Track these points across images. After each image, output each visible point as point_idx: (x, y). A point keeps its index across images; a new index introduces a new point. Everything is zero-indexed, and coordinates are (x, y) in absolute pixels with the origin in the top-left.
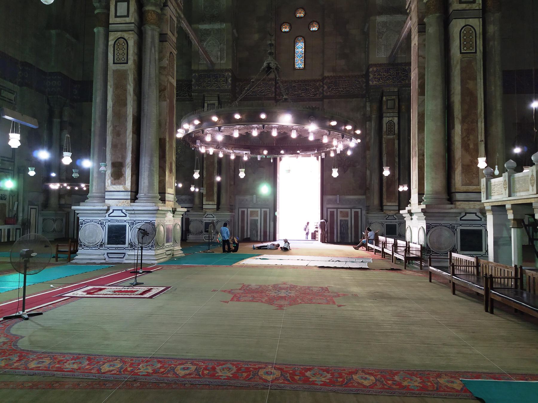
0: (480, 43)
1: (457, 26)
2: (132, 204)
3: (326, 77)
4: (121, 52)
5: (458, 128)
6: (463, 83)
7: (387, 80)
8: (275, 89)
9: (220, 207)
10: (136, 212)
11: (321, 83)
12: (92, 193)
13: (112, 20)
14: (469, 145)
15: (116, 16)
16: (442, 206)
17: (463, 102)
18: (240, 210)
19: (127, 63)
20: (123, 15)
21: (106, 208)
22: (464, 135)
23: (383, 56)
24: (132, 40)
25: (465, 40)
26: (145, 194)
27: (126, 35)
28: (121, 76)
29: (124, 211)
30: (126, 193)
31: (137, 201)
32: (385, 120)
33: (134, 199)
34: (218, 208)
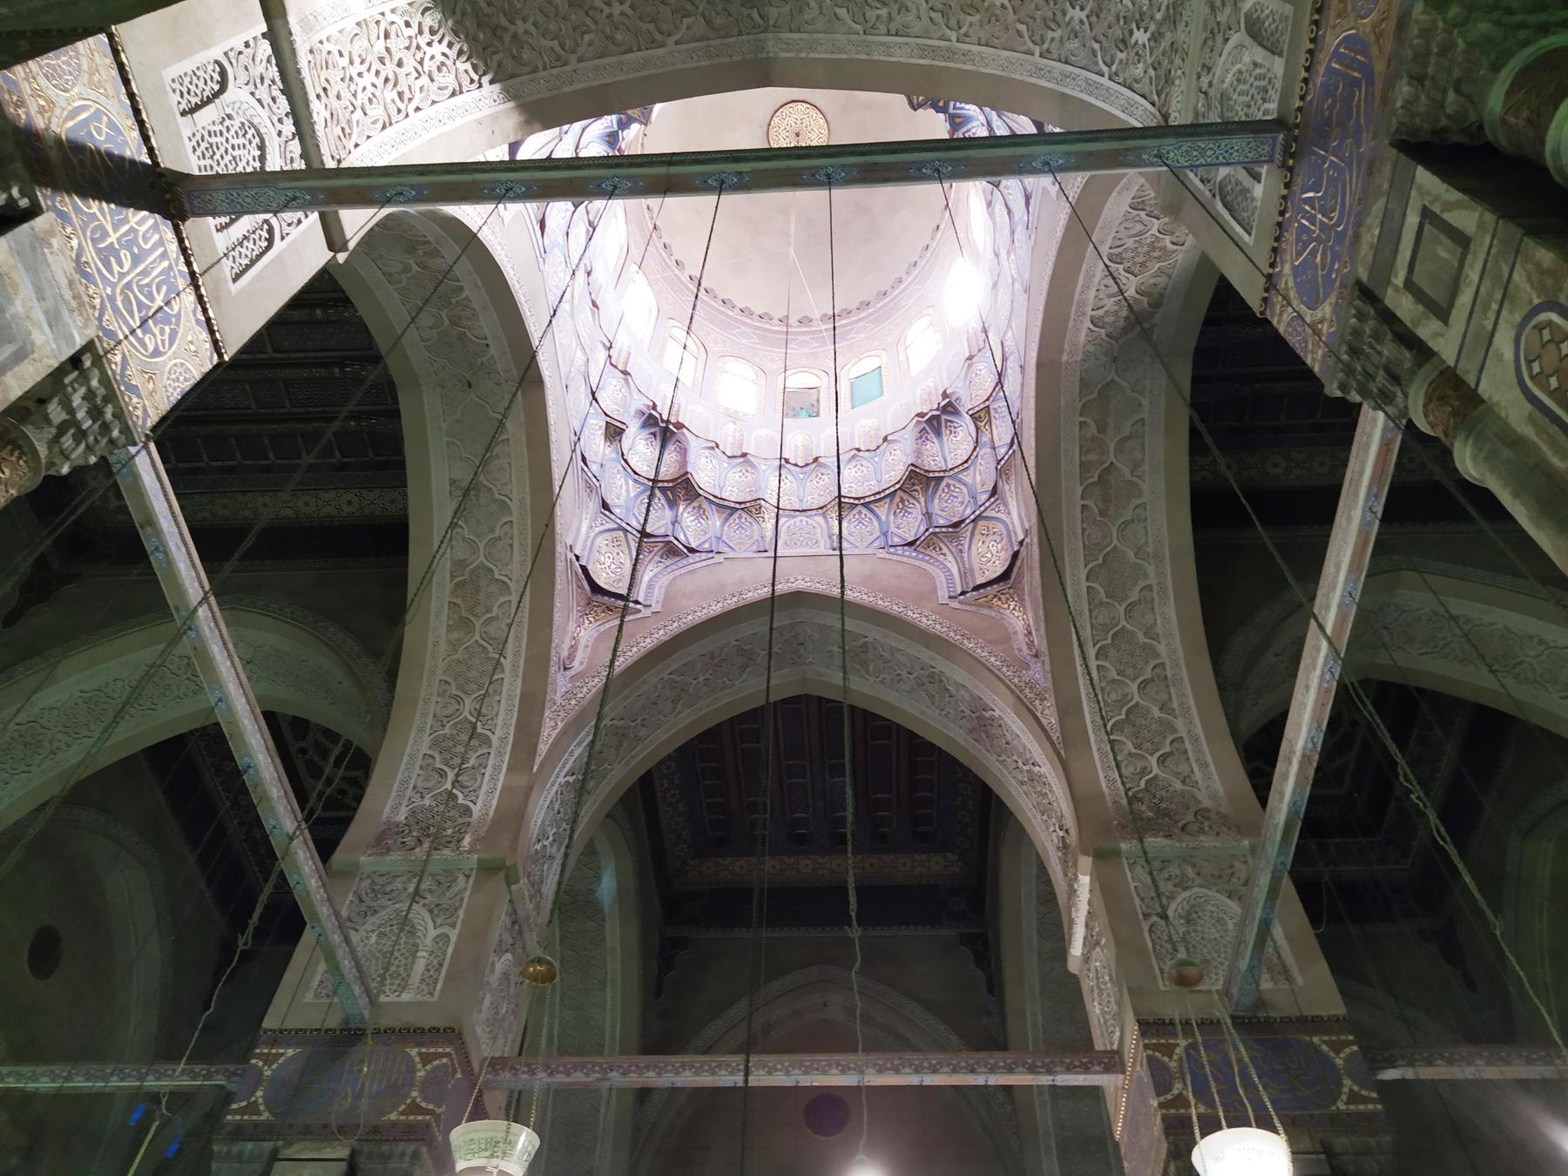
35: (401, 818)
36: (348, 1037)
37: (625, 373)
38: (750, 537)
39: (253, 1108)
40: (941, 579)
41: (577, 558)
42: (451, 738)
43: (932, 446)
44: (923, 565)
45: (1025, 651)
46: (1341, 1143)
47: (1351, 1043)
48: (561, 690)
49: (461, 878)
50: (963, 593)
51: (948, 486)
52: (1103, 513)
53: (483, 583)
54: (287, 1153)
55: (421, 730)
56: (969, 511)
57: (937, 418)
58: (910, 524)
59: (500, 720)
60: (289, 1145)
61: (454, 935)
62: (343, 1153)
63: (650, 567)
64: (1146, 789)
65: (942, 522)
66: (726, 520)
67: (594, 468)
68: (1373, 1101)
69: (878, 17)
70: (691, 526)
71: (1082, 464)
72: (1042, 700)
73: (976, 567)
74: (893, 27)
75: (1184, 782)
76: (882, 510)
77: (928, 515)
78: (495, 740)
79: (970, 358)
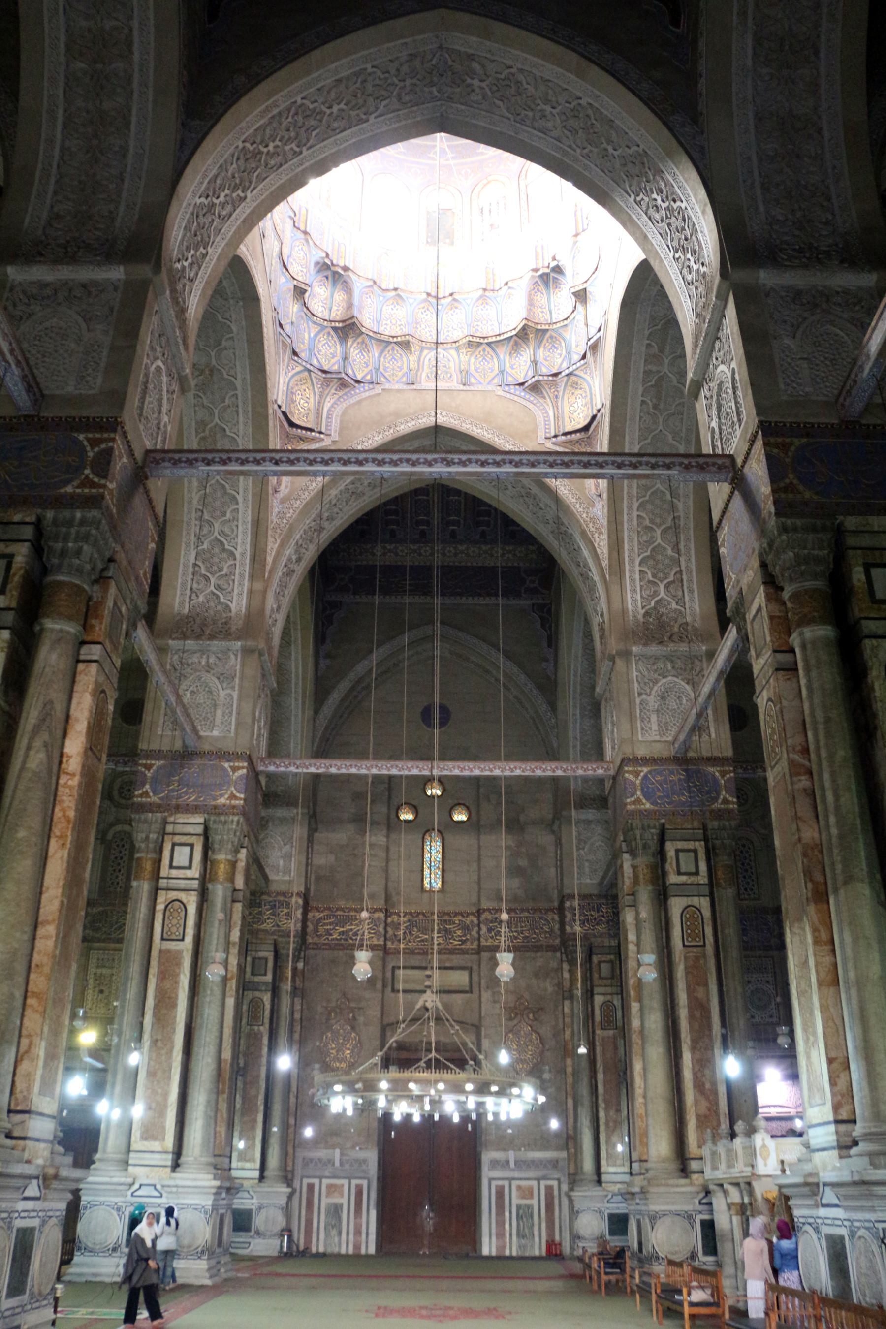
0: (709, 931)
1: (676, 905)
2: (174, 1175)
3: (484, 910)
4: (175, 922)
5: (687, 1058)
6: (690, 991)
7: (598, 924)
8: (385, 929)
9: (266, 1174)
10: (180, 1190)
11: (475, 920)
12: (104, 1151)
13: (164, 872)
14: (703, 1085)
15: (171, 867)
16: (671, 1182)
17: (691, 1017)
18: (306, 1181)
19: (183, 940)
20: (182, 865)
21: (130, 1180)
22: (696, 1069)
23: (588, 881)
24: (192, 902)
25: (688, 927)
26: (196, 1159)
27: (182, 896)
28: (170, 961)
29: (159, 1187)
30: (164, 1156)
31: (178, 1169)
32: (598, 1000)
33: (176, 1166)
34: (262, 1178)
35: (186, 611)
36: (186, 755)
37: (305, 233)
38: (401, 368)
39: (146, 794)
40: (540, 421)
41: (280, 407)
42: (209, 551)
43: (541, 299)
44: (531, 406)
45: (593, 491)
46: (713, 824)
47: (730, 772)
48: (276, 510)
49: (232, 656)
50: (555, 436)
51: (551, 337)
52: (655, 407)
53: (218, 436)
54: (171, 819)
55: (188, 545)
56: (564, 365)
57: (547, 275)
58: (520, 366)
59: (239, 541)
60: (171, 815)
61: (235, 695)
62: (200, 819)
63: (328, 399)
64: (655, 608)
65: (545, 371)
66: (382, 351)
67: (288, 328)
68: (733, 803)
69: (526, 116)
70: (360, 361)
71: (645, 372)
72: (600, 533)
73: (566, 415)
74: (536, 125)
75: (677, 603)
76: (502, 351)
77: (535, 363)
78: (237, 554)
79: (576, 235)
